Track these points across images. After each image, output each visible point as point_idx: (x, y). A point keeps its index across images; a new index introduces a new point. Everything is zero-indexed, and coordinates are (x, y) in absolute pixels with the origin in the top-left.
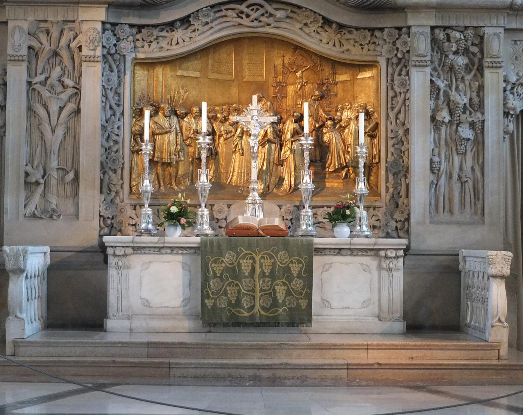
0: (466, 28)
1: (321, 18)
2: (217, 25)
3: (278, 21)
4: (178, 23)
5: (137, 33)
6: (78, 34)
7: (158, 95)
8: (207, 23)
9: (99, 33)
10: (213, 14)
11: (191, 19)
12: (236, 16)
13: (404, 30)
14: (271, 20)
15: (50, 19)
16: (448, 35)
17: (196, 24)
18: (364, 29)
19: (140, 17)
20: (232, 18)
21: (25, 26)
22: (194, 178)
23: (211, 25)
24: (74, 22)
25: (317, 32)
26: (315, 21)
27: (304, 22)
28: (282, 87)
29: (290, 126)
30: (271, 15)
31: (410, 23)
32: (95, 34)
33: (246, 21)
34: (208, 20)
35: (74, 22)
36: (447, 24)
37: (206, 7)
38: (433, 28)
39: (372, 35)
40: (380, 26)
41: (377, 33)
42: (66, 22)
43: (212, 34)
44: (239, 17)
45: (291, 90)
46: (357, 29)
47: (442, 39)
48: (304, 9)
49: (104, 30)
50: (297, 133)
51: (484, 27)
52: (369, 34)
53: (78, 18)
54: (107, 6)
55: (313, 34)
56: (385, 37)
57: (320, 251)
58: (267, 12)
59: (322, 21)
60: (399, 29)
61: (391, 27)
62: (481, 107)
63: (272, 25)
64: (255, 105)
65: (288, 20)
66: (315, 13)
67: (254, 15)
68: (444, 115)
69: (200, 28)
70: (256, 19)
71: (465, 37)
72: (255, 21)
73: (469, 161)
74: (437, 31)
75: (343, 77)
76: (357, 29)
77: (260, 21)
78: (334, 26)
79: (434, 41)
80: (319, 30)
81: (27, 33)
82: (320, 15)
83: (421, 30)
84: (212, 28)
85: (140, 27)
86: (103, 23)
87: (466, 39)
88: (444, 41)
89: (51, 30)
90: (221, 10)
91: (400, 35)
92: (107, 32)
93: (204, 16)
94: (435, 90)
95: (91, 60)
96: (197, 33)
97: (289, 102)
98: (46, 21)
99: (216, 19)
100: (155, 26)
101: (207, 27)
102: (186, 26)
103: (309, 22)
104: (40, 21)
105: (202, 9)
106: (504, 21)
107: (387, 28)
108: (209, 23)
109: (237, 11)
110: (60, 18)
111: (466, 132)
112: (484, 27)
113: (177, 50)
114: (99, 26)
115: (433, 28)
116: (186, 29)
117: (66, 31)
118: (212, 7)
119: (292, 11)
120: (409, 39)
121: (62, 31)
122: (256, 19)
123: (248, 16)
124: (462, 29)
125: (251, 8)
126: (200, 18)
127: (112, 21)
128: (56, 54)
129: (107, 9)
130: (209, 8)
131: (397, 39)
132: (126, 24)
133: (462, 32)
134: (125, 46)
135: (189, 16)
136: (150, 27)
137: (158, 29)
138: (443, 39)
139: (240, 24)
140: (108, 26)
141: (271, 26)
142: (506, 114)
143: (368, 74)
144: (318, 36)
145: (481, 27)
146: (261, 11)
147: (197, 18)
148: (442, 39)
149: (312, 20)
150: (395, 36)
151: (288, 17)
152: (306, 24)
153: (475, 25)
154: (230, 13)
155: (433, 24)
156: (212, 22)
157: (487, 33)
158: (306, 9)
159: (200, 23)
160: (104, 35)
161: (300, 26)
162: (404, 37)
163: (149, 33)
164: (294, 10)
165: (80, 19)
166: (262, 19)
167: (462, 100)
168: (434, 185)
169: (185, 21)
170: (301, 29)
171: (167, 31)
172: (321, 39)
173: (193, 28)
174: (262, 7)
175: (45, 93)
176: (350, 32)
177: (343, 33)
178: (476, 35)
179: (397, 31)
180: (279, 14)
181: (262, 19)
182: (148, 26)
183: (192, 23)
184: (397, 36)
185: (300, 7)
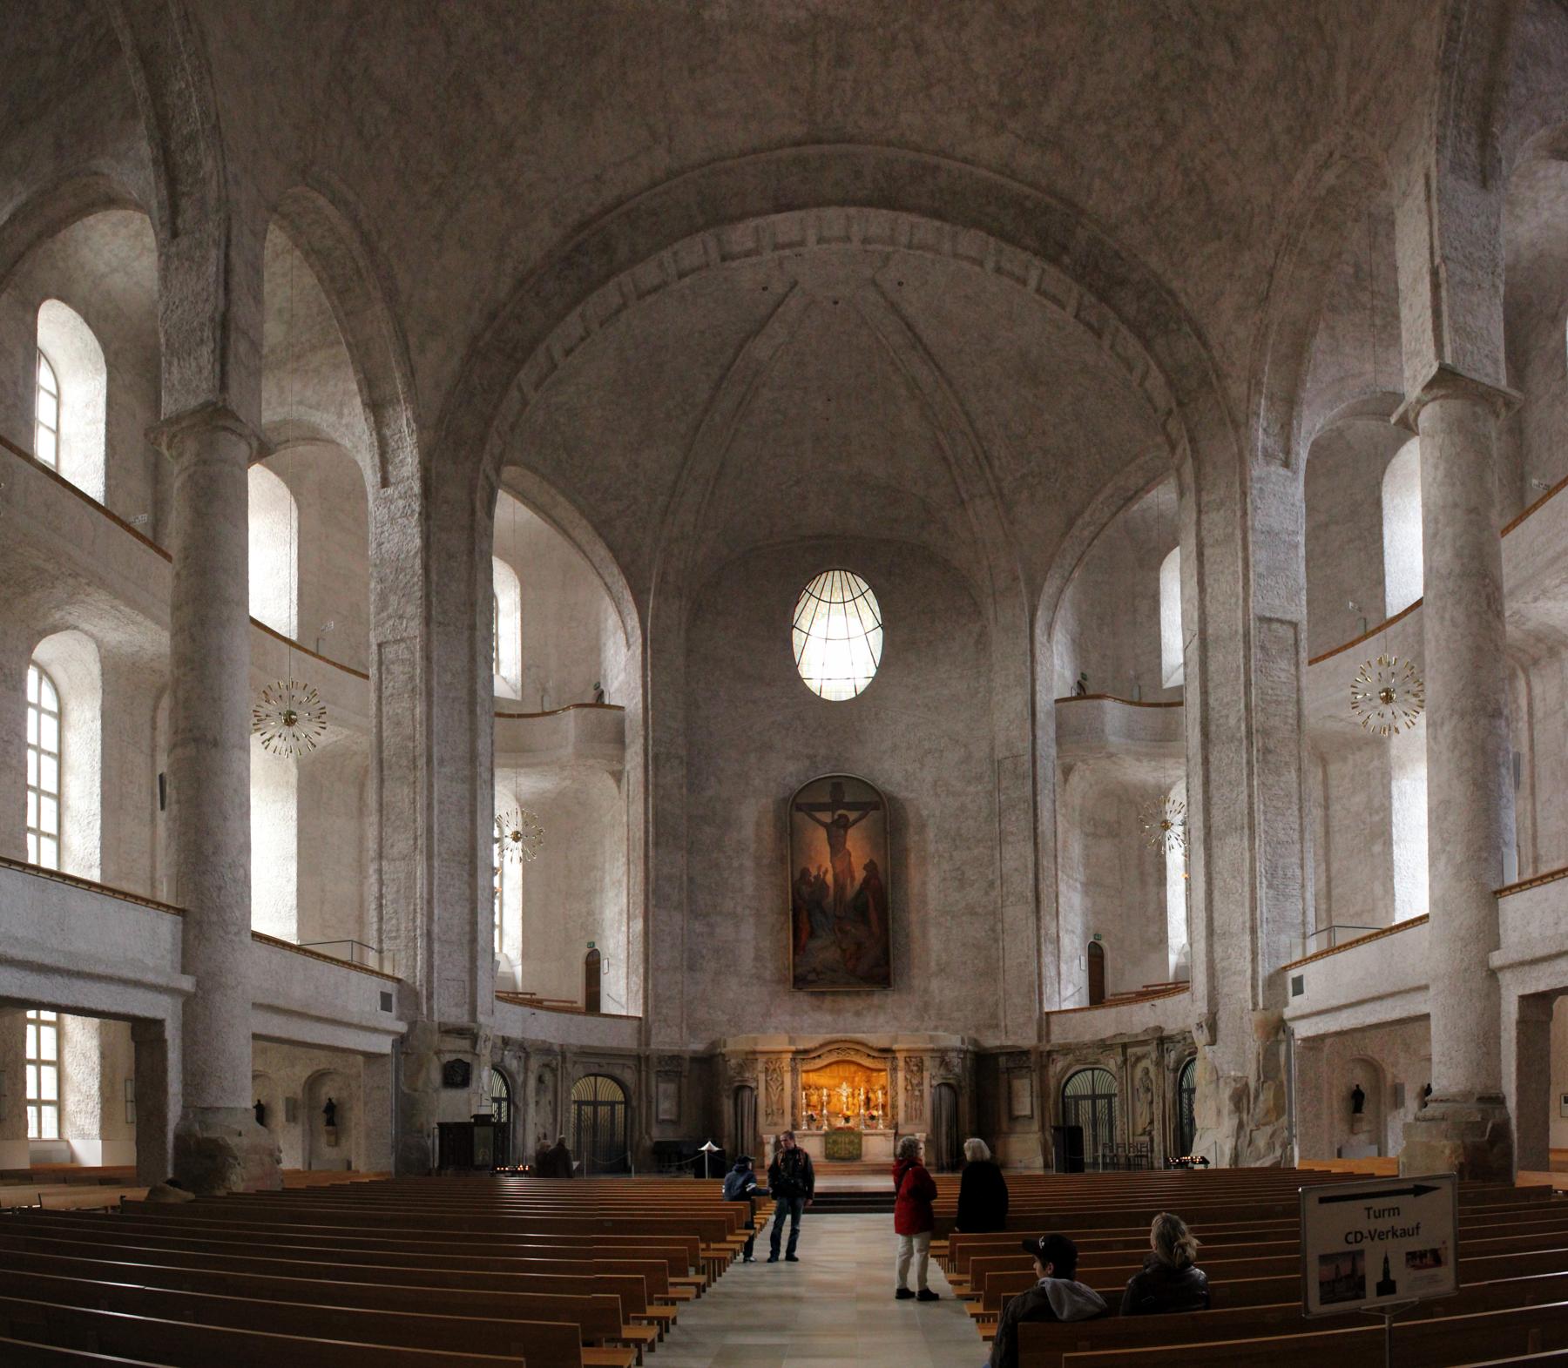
7: (811, 1082)
21: (764, 1060)
22: (822, 1110)
28: (854, 1078)
29: (857, 1092)
45: (857, 1079)
50: (859, 1094)
57: (866, 1135)
62: (922, 1084)
64: (844, 1085)
68: (909, 1087)
73: (918, 1103)
75: (875, 1074)
79: (906, 1062)
85: (803, 1059)
94: (906, 1079)
95: (787, 1071)
97: (856, 1084)
106: (930, 1054)
111: (917, 1093)
113: (819, 1066)
128: (775, 1070)
134: (799, 1066)
142: (931, 1086)
143: (883, 1073)
167: (915, 1082)
168: (906, 1111)
169: (819, 1056)
175: (771, 1083)
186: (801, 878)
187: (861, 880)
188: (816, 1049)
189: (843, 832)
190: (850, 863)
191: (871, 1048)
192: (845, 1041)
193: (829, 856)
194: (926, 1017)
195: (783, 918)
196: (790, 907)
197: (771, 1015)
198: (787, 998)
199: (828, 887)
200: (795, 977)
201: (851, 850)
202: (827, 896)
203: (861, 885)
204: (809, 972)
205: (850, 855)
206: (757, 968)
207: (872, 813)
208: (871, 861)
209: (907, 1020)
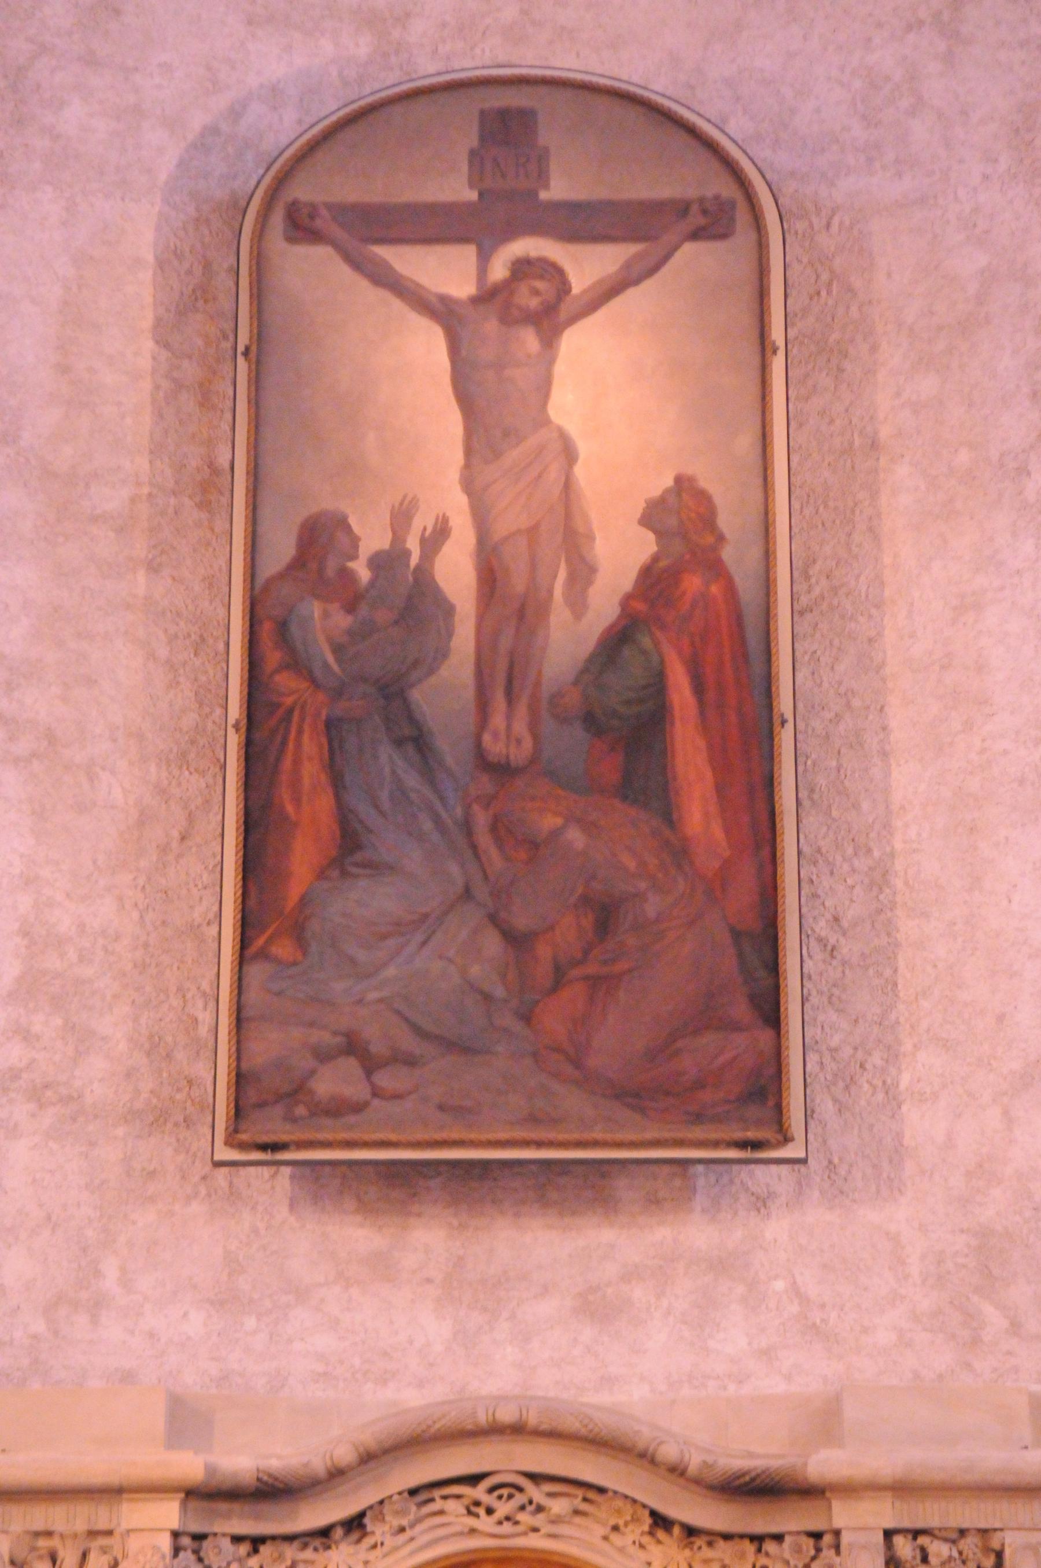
0: (963, 1532)
1: (647, 1513)
2: (423, 1532)
3: (555, 1521)
4: (339, 1532)
5: (249, 1555)
6: (120, 1559)
8: (402, 1530)
9: (163, 1557)
10: (414, 1508)
11: (367, 1520)
12: (465, 1512)
13: (827, 1539)
14: (539, 1520)
15: (59, 1527)
16: (923, 1550)
17: (378, 1531)
18: (742, 1536)
19: (258, 1517)
20: (457, 1516)
23: (409, 1533)
24: (109, 1533)
25: (642, 1546)
26: (635, 1520)
27: (612, 1522)
30: (540, 1509)
31: (838, 1522)
32: (155, 1558)
33: (485, 1523)
34: (405, 1522)
35: (109, 1533)
36: (920, 1525)
37: (400, 1493)
38: (889, 1534)
39: (759, 1550)
40: (774, 1529)
41: (770, 1546)
42: (92, 1534)
43: (412, 1553)
44: (470, 1513)
46: (727, 1537)
47: (909, 1558)
48: (610, 1494)
49: (177, 1550)
51: (1001, 1530)
52: (750, 1548)
53: (119, 1524)
54: (182, 1495)
55: (633, 1550)
56: (787, 1555)
58: (531, 1502)
59: (648, 1521)
60: (817, 1536)
61: (798, 1533)
63: (543, 1531)
65: (578, 1520)
66: (634, 1501)
67: (503, 1509)
69: (390, 1542)
70: (508, 1518)
71: (960, 1553)
72: (505, 1523)
74: (899, 1541)
76: (727, 1537)
77: (517, 1523)
78: (676, 1530)
80: (646, 1540)
81: (7, 1559)
82: (644, 1506)
83: (862, 1538)
84: (412, 1539)
85: (257, 1542)
86: (176, 1535)
87: (964, 1557)
88: (914, 1563)
89: (61, 1554)
90: (432, 1500)
91: (818, 1550)
92: (182, 1554)
93: (397, 1513)
96: (378, 1551)
98: (49, 1534)
99: (419, 1520)
100: (290, 1538)
101: (402, 1538)
102: (355, 1536)
103: (621, 1522)
104: (37, 1534)
105: (391, 1497)
107: (790, 1533)
108: (407, 1529)
109: (466, 1501)
110: (80, 1526)
112: (1001, 1530)
114: (165, 1543)
115: (889, 1534)
116: (359, 1541)
117: (92, 1557)
118: (413, 1492)
119: (585, 1500)
120: (837, 1560)
121: (84, 1555)
122: (508, 1518)
123: (490, 1511)
124: (954, 1535)
125: (496, 1493)
126: (388, 1518)
127: (195, 1528)
129: (184, 1504)
130: (406, 1495)
131: (813, 1558)
132: (224, 1535)
133: (954, 1542)
135: (362, 1515)
136: (278, 1542)
137: (296, 1544)
138: (914, 1558)
139: (473, 1531)
140: (186, 1541)
141: (538, 1534)
144: (642, 1555)
145: (995, 1530)
146: (519, 1499)
147: (381, 1518)
148: (909, 1558)
149: (629, 1518)
150: (808, 1551)
151: (577, 1512)
152: (615, 1528)
153: (983, 1525)
154: (451, 1505)
155: (890, 1525)
156: (412, 1526)
157: (1010, 1546)
158: (615, 1492)
159: (386, 1528)
160: (176, 1561)
161: (601, 1531)
162: (828, 1554)
163: (276, 1555)
164: (591, 1495)
165: (124, 1526)
166: (521, 1517)
169: (355, 1525)
170: (605, 1538)
171: (316, 1549)
172: (649, 1560)
173: (369, 1541)
174: (520, 1489)
176: (710, 1544)
177: (695, 1547)
178: (987, 1550)
179: (811, 1542)
180: (558, 1507)
181: (521, 1517)
182: (274, 1538)
183: (369, 1528)
184: (812, 1552)
185: (601, 1490)
186: (299, 563)
187: (627, 583)
188: (337, 1474)
189: (530, 340)
190: (568, 485)
191: (677, 1471)
192: (517, 1430)
193: (458, 456)
194: (994, 1319)
195: (194, 784)
196: (235, 710)
197: (97, 1306)
198: (196, 1207)
199: (449, 610)
200: (240, 1079)
201: (572, 429)
202: (443, 653)
203: (627, 601)
204: (323, 1056)
205: (569, 454)
206: (27, 1037)
207: (689, 248)
208: (683, 483)
209: (884, 1337)
